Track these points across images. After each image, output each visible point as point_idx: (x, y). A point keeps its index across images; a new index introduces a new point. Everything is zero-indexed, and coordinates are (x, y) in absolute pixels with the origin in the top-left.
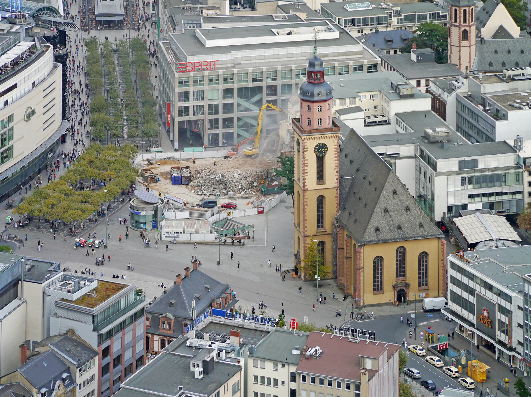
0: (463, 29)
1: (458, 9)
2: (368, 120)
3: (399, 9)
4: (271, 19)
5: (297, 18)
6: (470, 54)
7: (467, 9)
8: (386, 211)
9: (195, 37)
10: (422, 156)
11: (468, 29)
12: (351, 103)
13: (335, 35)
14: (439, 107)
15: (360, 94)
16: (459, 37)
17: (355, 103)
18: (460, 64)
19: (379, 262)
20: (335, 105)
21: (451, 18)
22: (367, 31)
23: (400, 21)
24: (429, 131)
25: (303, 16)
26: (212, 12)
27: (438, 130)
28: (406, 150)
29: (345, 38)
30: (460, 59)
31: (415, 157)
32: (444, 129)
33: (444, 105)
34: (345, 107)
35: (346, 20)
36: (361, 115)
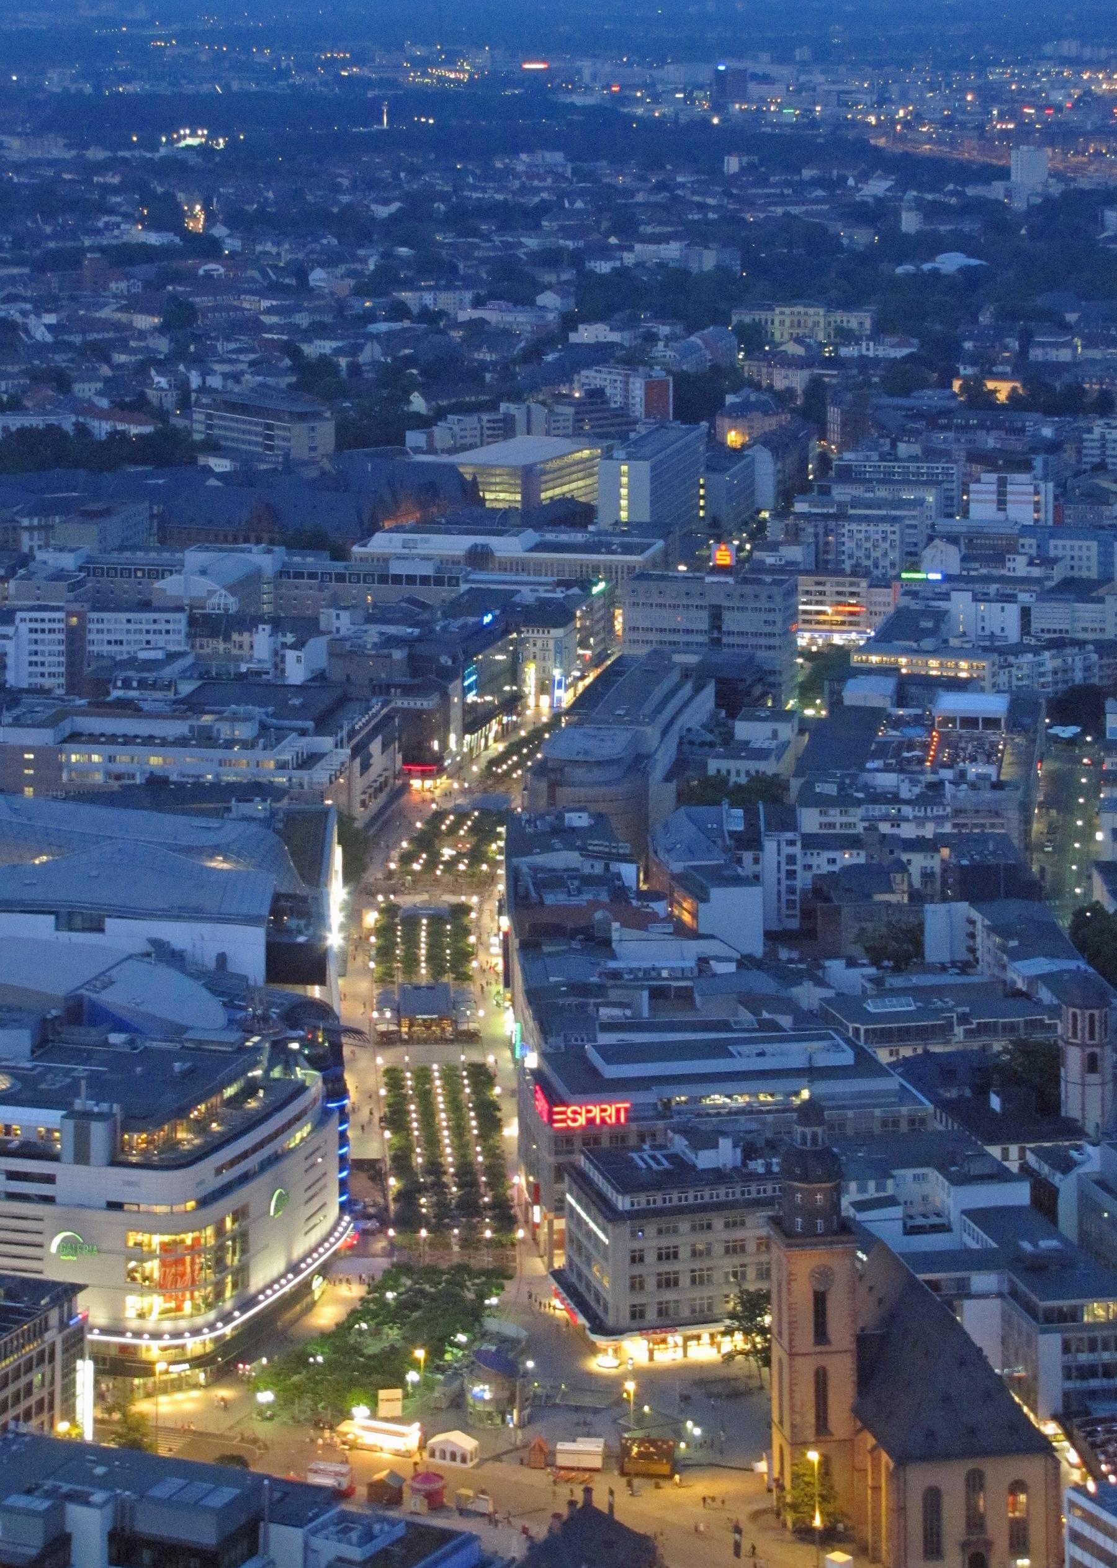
0: (1089, 1050)
1: (1078, 1011)
2: (910, 1223)
3: (967, 1010)
4: (725, 1026)
5: (774, 1026)
6: (1103, 1099)
7: (1096, 1012)
8: (947, 1399)
9: (583, 1058)
10: (1014, 1294)
11: (1097, 1050)
12: (877, 1190)
13: (847, 1058)
14: (1045, 1200)
15: (895, 1172)
16: (1083, 1065)
17: (884, 1190)
18: (1084, 1118)
19: (933, 1499)
20: (847, 1192)
21: (1066, 1029)
22: (906, 1052)
23: (968, 1032)
24: (1027, 1246)
25: (786, 1021)
26: (616, 1012)
27: (1043, 1244)
28: (982, 1281)
29: (865, 1065)
30: (1083, 1109)
31: (1000, 1295)
32: (1054, 1243)
33: (1054, 1193)
34: (866, 1196)
35: (866, 1031)
36: (897, 1212)
